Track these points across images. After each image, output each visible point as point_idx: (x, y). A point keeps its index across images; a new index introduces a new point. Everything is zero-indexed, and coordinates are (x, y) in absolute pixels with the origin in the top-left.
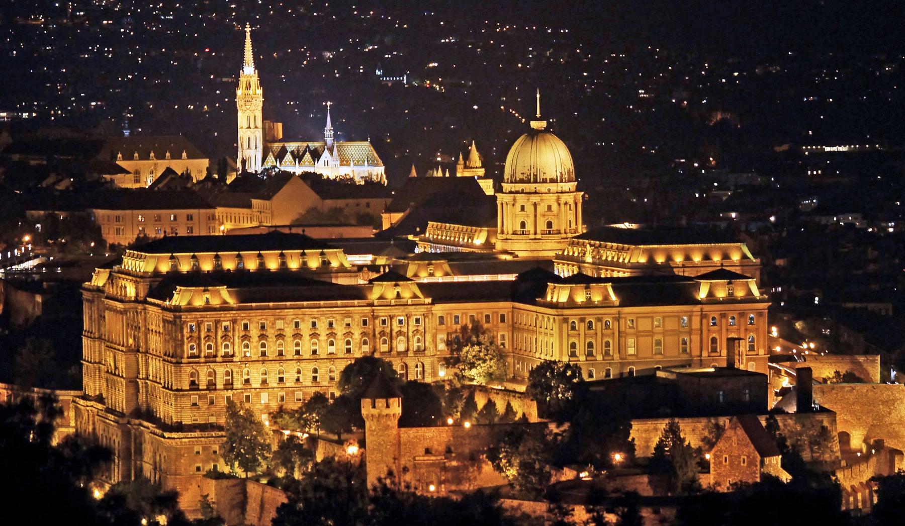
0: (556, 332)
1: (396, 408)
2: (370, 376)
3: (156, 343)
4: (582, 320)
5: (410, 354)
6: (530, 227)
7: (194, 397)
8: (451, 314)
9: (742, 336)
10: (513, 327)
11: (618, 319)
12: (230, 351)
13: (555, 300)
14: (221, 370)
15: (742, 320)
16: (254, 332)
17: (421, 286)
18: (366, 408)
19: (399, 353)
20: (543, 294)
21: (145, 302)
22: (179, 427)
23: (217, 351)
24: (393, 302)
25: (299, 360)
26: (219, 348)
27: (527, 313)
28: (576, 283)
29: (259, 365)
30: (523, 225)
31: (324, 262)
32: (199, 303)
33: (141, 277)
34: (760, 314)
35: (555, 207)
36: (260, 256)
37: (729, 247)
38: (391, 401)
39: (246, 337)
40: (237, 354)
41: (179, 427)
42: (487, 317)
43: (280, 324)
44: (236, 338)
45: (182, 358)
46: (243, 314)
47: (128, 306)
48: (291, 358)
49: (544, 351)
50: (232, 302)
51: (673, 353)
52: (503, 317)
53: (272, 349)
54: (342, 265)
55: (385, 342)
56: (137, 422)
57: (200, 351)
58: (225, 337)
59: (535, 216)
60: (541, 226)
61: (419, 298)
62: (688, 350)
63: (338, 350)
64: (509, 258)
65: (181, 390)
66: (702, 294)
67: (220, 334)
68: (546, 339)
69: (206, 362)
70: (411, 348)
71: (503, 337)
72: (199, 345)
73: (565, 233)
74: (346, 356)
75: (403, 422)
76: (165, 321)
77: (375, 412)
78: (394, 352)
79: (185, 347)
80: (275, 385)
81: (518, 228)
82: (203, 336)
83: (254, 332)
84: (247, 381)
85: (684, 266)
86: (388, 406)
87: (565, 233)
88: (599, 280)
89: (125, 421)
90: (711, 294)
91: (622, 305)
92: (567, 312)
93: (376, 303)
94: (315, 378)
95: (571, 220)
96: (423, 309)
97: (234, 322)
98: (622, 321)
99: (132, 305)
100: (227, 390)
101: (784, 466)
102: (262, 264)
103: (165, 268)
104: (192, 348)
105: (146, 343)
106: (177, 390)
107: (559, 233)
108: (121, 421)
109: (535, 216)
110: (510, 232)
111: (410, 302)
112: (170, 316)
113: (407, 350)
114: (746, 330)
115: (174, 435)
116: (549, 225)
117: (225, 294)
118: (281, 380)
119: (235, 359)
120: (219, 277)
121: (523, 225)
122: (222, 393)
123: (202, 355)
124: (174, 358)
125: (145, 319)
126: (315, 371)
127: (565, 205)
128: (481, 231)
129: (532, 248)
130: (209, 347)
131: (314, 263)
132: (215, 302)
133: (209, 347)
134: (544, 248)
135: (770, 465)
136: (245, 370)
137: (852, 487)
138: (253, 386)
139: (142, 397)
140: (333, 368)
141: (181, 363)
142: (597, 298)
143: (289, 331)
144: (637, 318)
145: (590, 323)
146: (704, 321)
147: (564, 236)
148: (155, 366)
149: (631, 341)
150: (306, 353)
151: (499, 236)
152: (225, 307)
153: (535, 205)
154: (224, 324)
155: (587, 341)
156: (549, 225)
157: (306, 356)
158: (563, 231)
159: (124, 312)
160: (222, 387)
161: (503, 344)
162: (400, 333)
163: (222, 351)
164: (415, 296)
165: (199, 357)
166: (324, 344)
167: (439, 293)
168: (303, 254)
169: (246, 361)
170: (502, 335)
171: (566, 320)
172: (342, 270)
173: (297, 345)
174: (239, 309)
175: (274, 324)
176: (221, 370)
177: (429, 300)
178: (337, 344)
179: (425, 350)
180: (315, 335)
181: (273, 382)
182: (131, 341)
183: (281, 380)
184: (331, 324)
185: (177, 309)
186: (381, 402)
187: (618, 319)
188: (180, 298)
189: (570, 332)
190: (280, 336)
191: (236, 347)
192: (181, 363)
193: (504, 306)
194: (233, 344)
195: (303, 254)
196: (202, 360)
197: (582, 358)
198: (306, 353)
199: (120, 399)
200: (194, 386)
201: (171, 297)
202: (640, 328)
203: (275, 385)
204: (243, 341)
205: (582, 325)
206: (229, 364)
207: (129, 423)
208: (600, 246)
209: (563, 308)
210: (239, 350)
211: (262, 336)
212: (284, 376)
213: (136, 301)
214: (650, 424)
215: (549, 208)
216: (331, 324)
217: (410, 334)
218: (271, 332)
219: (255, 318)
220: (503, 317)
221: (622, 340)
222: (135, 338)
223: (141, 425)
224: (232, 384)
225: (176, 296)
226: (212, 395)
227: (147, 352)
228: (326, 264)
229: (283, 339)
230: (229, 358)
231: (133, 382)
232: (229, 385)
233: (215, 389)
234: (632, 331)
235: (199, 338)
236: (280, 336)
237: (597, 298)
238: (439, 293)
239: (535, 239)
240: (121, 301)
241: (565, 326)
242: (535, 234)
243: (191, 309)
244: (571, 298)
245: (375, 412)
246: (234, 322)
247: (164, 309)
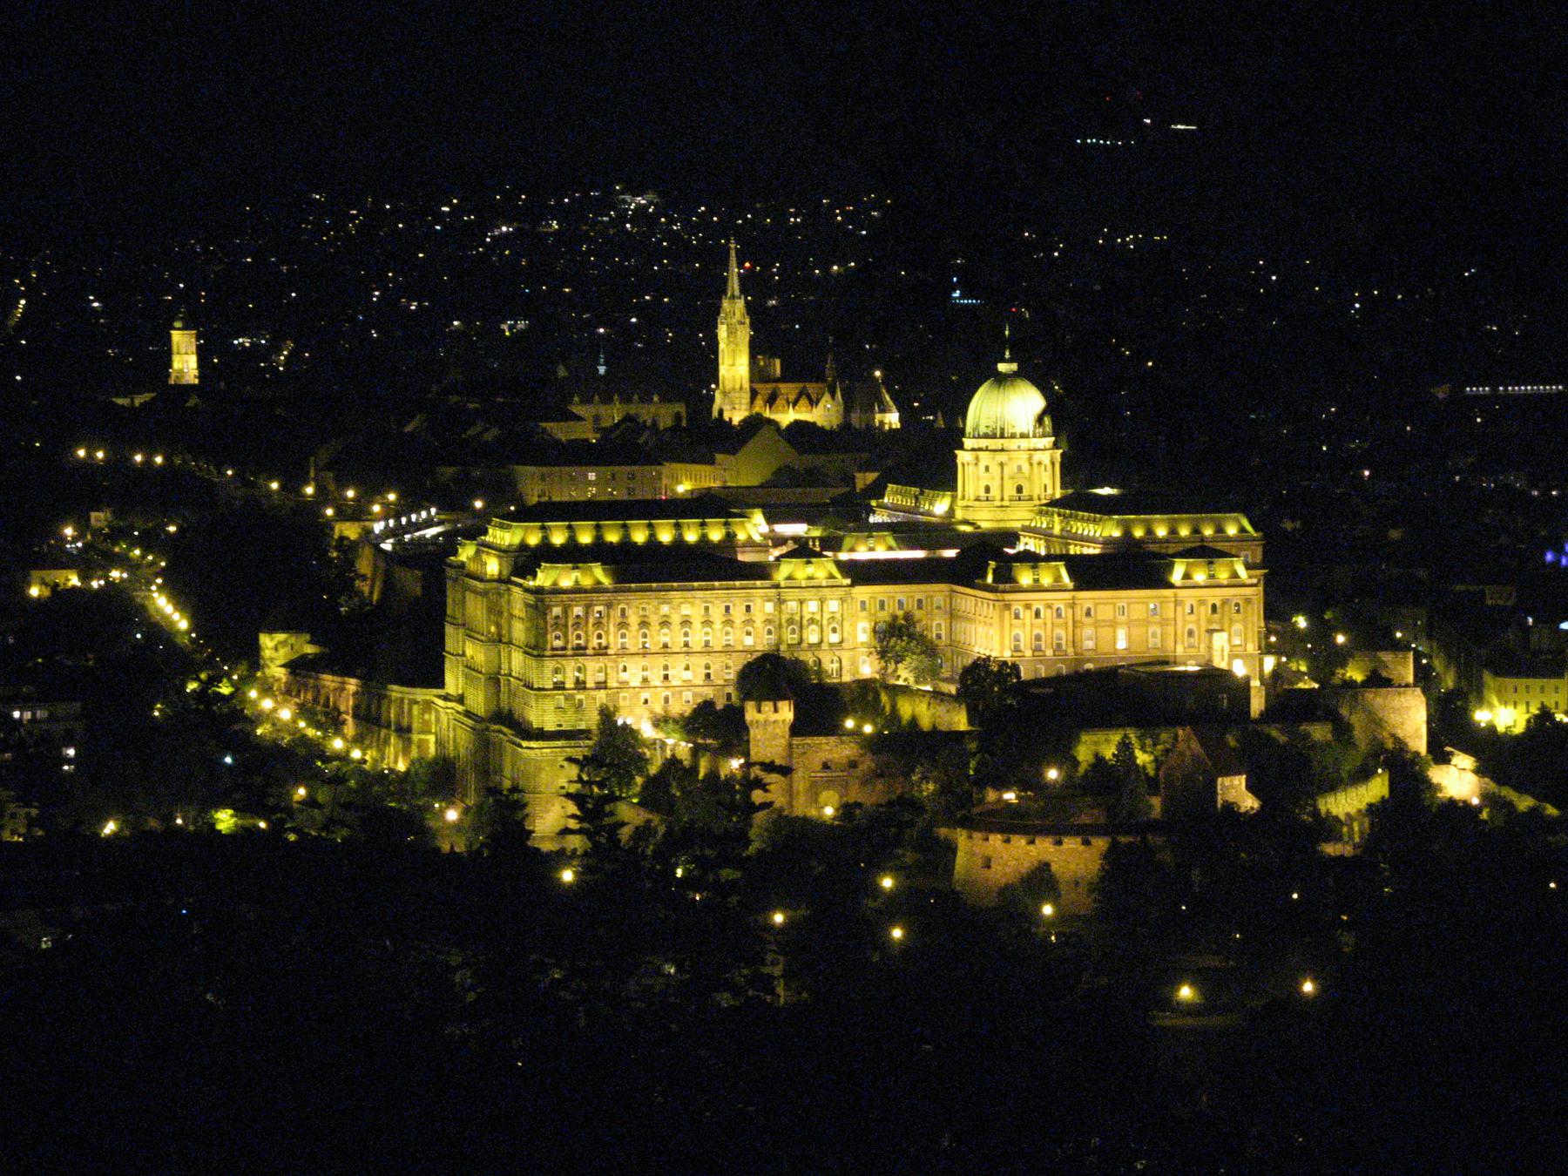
0: (996, 620)
1: (786, 712)
2: (771, 674)
3: (519, 631)
4: (1028, 607)
5: (825, 646)
7: (560, 698)
11: (1073, 606)
12: (604, 642)
17: (840, 565)
18: (751, 714)
19: (811, 645)
21: (509, 582)
22: (541, 735)
24: (804, 584)
27: (969, 600)
29: (639, 659)
30: (987, 490)
31: (728, 534)
32: (567, 582)
33: (504, 551)
34: (1248, 601)
35: (1026, 468)
36: (543, 528)
38: (780, 704)
39: (623, 625)
41: (541, 735)
42: (920, 601)
43: (665, 609)
46: (620, 597)
47: (488, 586)
50: (606, 581)
51: (1007, 655)
54: (750, 537)
55: (793, 632)
56: (497, 727)
57: (567, 642)
58: (598, 624)
60: (1010, 491)
66: (1176, 576)
67: (591, 621)
71: (939, 625)
72: (566, 635)
75: (797, 729)
76: (527, 605)
77: (760, 717)
78: (804, 645)
80: (659, 684)
81: (982, 494)
83: (633, 620)
86: (776, 710)
88: (1049, 558)
89: (483, 726)
90: (1187, 576)
91: (1076, 589)
93: (783, 584)
94: (708, 676)
95: (1047, 481)
96: (840, 592)
98: (1078, 609)
99: (495, 585)
101: (1249, 788)
102: (545, 538)
103: (534, 540)
105: (510, 632)
107: (1031, 499)
108: (479, 726)
112: (531, 599)
113: (821, 642)
115: (533, 744)
116: (1019, 489)
117: (598, 573)
118: (666, 677)
120: (599, 552)
121: (987, 490)
124: (536, 650)
125: (509, 602)
126: (708, 667)
131: (716, 535)
132: (587, 582)
133: (579, 637)
135: (1232, 786)
137: (1348, 814)
139: (504, 697)
140: (730, 663)
142: (1046, 580)
148: (517, 661)
149: (1088, 631)
152: (598, 589)
153: (1002, 465)
154: (598, 608)
155: (1036, 632)
156: (1019, 489)
159: (484, 594)
161: (939, 637)
162: (812, 621)
163: (594, 642)
164: (831, 577)
166: (718, 634)
167: (863, 573)
168: (703, 525)
169: (623, 652)
170: (935, 627)
171: (1008, 607)
172: (750, 544)
173: (686, 634)
174: (616, 591)
175: (657, 609)
177: (848, 581)
181: (656, 679)
182: (493, 629)
183: (666, 677)
184: (727, 608)
185: (539, 591)
186: (767, 706)
187: (1073, 606)
188: (544, 578)
193: (937, 592)
194: (607, 633)
195: (625, 526)
196: (570, 652)
197: (1028, 653)
199: (478, 701)
200: (559, 686)
201: (535, 576)
203: (659, 684)
207: (487, 729)
210: (613, 640)
211: (644, 624)
213: (500, 580)
214: (1099, 736)
215: (1020, 468)
216: (727, 608)
218: (654, 620)
219: (639, 605)
222: (499, 626)
223: (500, 731)
225: (540, 574)
226: (580, 696)
227: (510, 643)
228: (730, 537)
231: (494, 680)
234: (1088, 620)
235: (566, 626)
236: (665, 623)
237: (1046, 580)
238: (863, 573)
240: (481, 580)
243: (556, 591)
245: (760, 717)
247: (527, 590)
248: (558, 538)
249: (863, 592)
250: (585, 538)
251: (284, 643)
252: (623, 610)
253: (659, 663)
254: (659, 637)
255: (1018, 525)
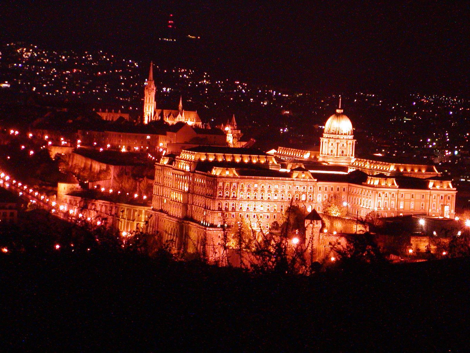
5: (307, 202)
6: (335, 152)
8: (324, 186)
9: (445, 204)
10: (348, 193)
12: (235, 195)
13: (372, 183)
14: (231, 203)
15: (438, 197)
16: (246, 188)
19: (303, 201)
20: (366, 181)
23: (230, 195)
25: (262, 201)
26: (231, 194)
28: (382, 177)
29: (246, 202)
30: (332, 151)
34: (453, 196)
35: (345, 145)
37: (422, 167)
40: (238, 197)
43: (256, 186)
44: (238, 190)
45: (216, 197)
46: (242, 180)
48: (259, 200)
49: (365, 204)
52: (344, 189)
53: (252, 195)
58: (234, 189)
59: (337, 148)
60: (340, 153)
61: (311, 178)
62: (424, 209)
63: (278, 198)
64: (326, 164)
65: (214, 210)
67: (232, 188)
68: (367, 199)
69: (226, 199)
70: (307, 199)
73: (349, 156)
74: (281, 201)
79: (218, 192)
81: (330, 152)
82: (225, 189)
83: (246, 188)
84: (241, 208)
85: (411, 173)
87: (349, 156)
92: (378, 189)
95: (350, 150)
96: (314, 183)
97: (238, 183)
100: (233, 211)
104: (220, 193)
105: (193, 189)
106: (213, 210)
107: (346, 156)
109: (337, 148)
110: (326, 154)
111: (308, 180)
113: (306, 200)
114: (447, 202)
116: (343, 152)
118: (255, 209)
119: (237, 199)
121: (332, 151)
122: (231, 213)
123: (224, 196)
127: (348, 145)
128: (307, 152)
129: (336, 161)
130: (227, 193)
134: (340, 161)
136: (240, 204)
138: (243, 211)
141: (215, 199)
143: (259, 189)
144: (405, 194)
145: (393, 195)
146: (431, 197)
147: (348, 157)
150: (265, 199)
151: (320, 155)
153: (338, 144)
156: (343, 152)
157: (266, 200)
158: (348, 155)
160: (231, 210)
165: (222, 197)
171: (377, 192)
175: (254, 185)
176: (231, 203)
177: (316, 180)
178: (278, 195)
179: (313, 200)
180: (269, 191)
183: (255, 209)
189: (378, 198)
190: (256, 190)
191: (238, 194)
192: (215, 199)
193: (345, 185)
198: (265, 199)
202: (406, 198)
203: (252, 211)
204: (241, 192)
205: (383, 195)
206: (234, 201)
207: (183, 222)
208: (360, 160)
209: (376, 187)
210: (239, 195)
211: (248, 190)
212: (256, 207)
215: (343, 145)
217: (308, 193)
218: (252, 189)
220: (344, 189)
221: (399, 202)
224: (235, 209)
229: (257, 192)
230: (234, 198)
232: (234, 209)
233: (228, 211)
235: (223, 189)
239: (337, 157)
241: (377, 194)
242: (337, 155)
243: (221, 177)
244: (379, 183)
246: (238, 183)
249: (320, 184)
252: (242, 186)
255: (347, 164)
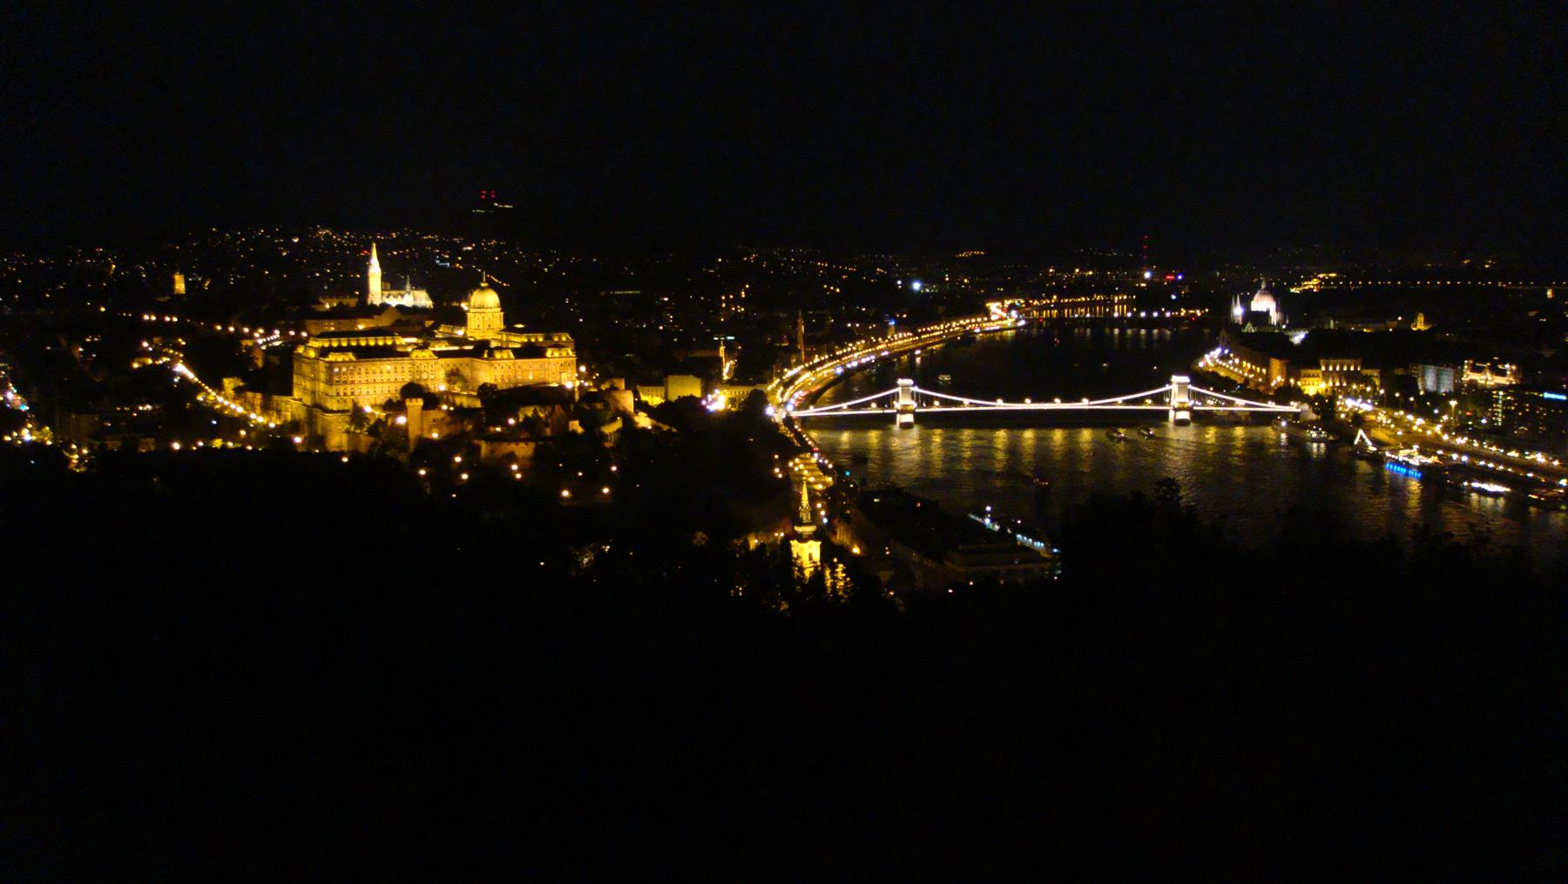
1: (420, 402)
2: (412, 389)
3: (323, 376)
18: (408, 403)
27: (478, 362)
66: (549, 353)
75: (425, 408)
95: (499, 323)
117: (351, 356)
124: (329, 382)
131: (389, 342)
148: (322, 387)
167: (441, 355)
170: (466, 372)
188: (332, 357)
193: (467, 360)
199: (308, 400)
210: (356, 378)
231: (313, 393)
238: (441, 355)
248: (335, 344)
249: (443, 361)
250: (344, 344)
251: (1012, 307)
253: (373, 387)
254: (371, 377)
